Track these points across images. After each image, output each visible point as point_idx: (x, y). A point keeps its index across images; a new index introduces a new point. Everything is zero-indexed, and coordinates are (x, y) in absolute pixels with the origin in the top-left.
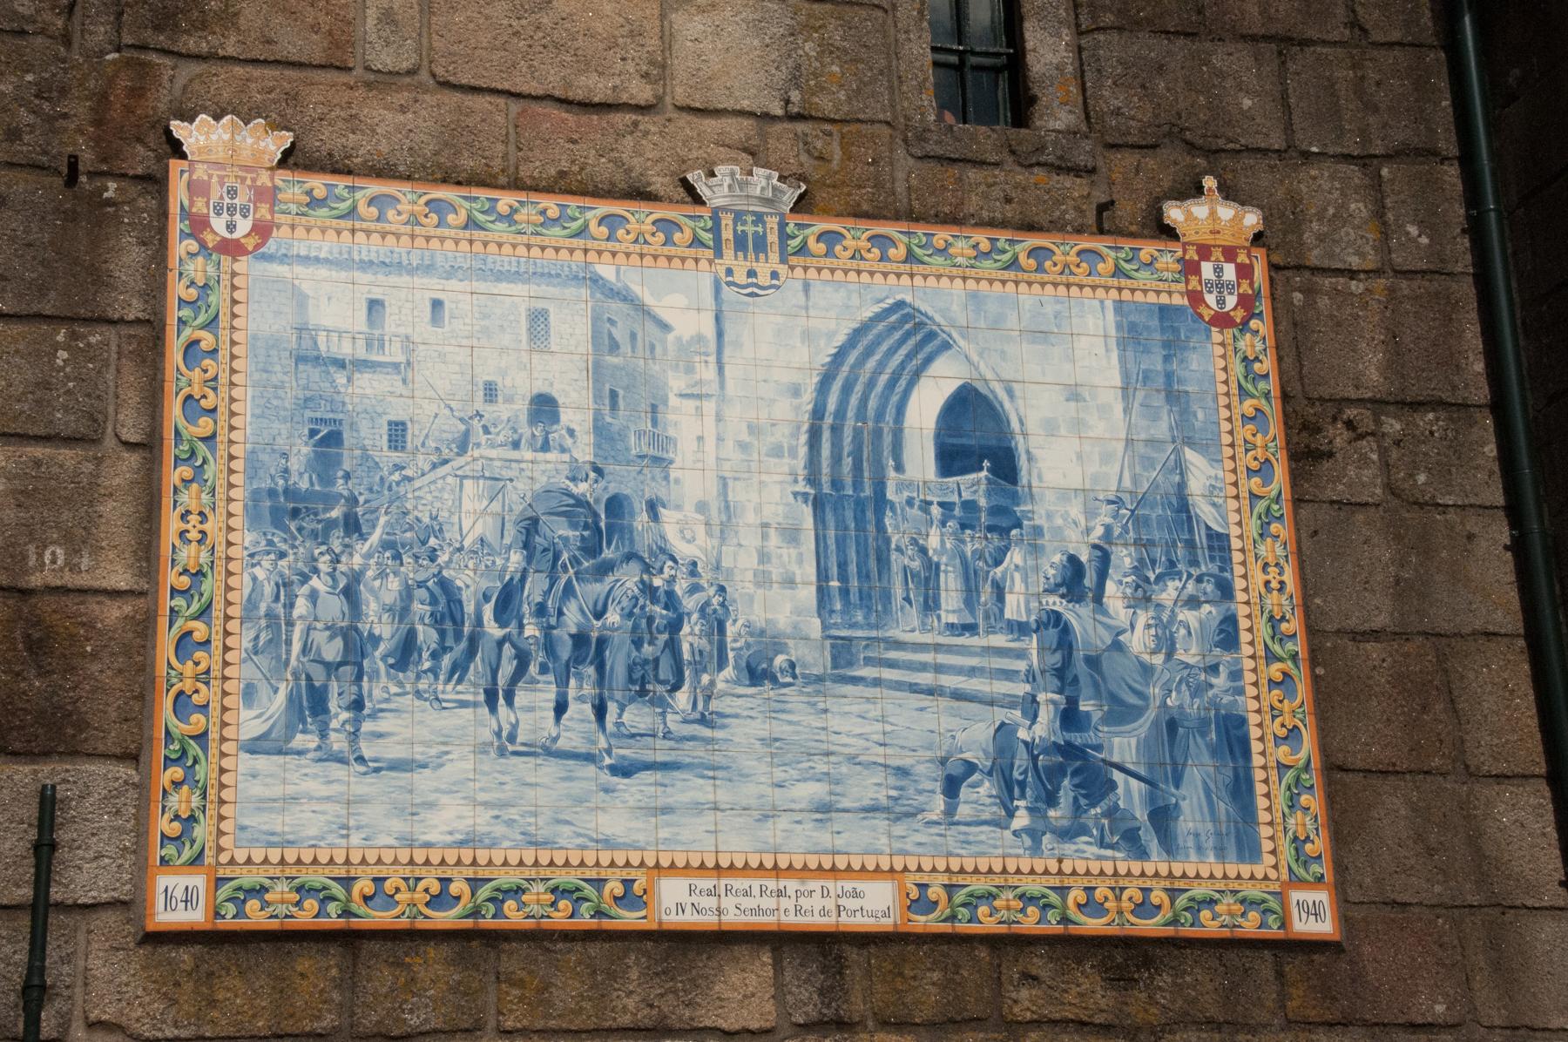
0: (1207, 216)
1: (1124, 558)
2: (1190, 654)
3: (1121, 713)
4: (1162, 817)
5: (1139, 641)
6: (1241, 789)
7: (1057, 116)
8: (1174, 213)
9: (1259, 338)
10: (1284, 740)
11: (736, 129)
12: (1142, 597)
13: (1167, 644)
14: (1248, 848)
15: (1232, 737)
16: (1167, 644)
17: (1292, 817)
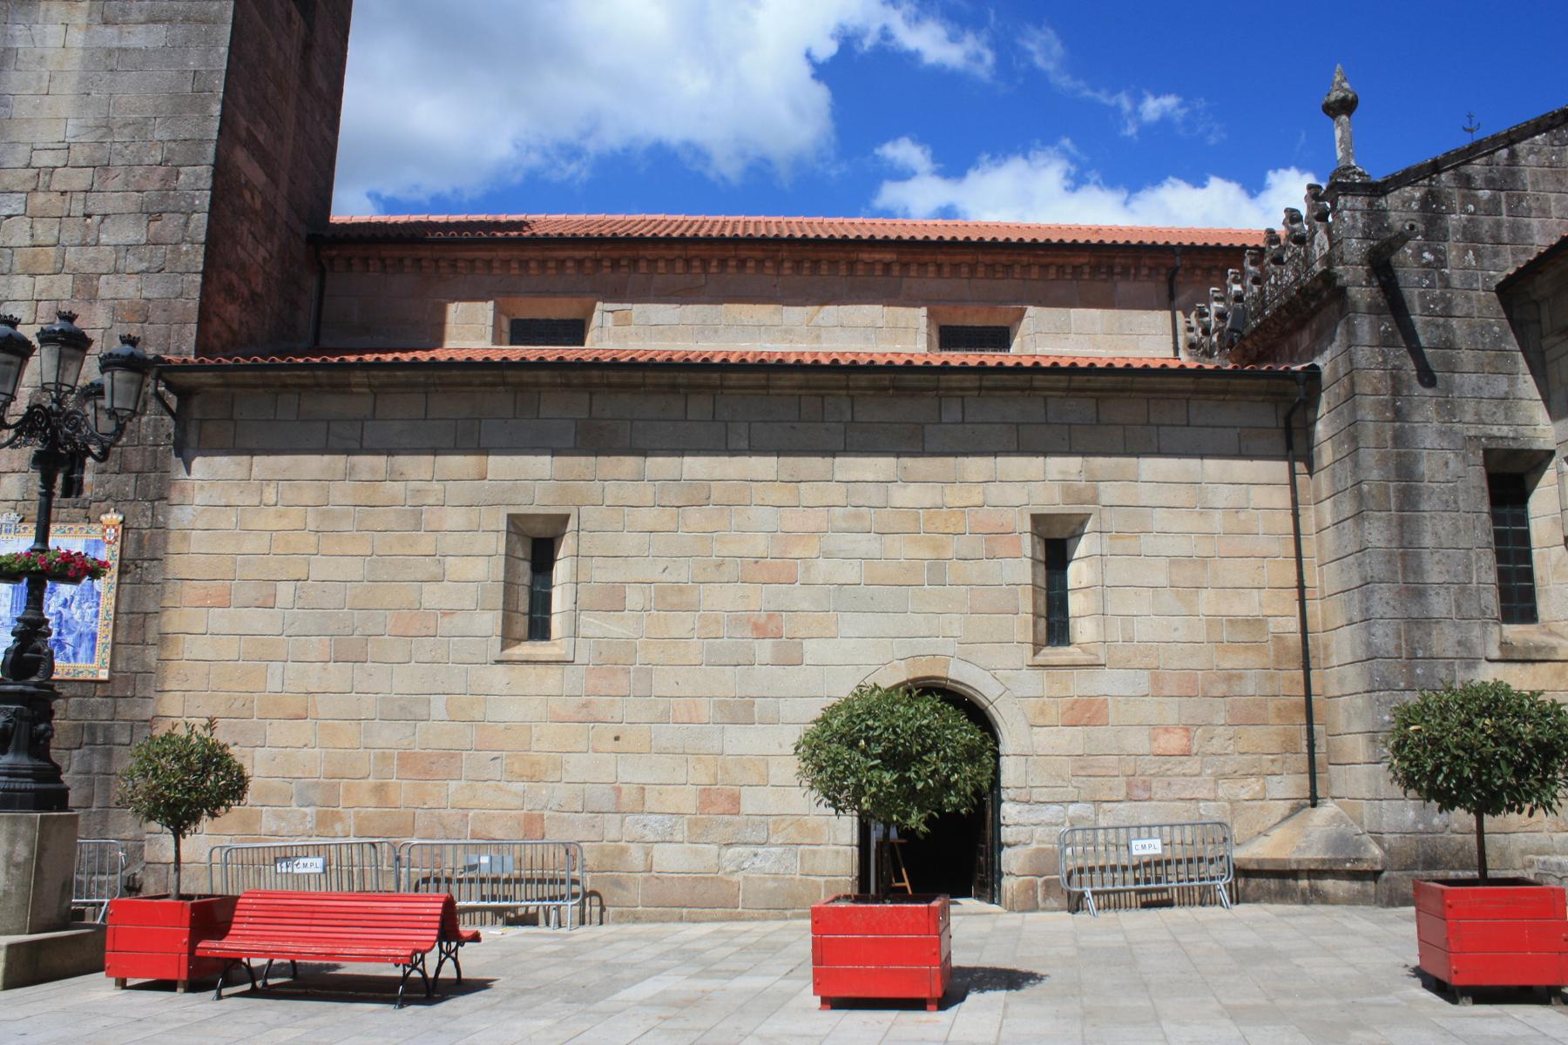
0: (113, 518)
1: (77, 598)
2: (87, 619)
3: (70, 632)
4: (75, 654)
5: (77, 617)
6: (93, 649)
7: (87, 493)
8: (103, 518)
9: (116, 548)
10: (104, 636)
11: (12, 504)
12: (79, 607)
13: (83, 617)
14: (92, 661)
15: (94, 637)
16: (83, 617)
17: (103, 654)
